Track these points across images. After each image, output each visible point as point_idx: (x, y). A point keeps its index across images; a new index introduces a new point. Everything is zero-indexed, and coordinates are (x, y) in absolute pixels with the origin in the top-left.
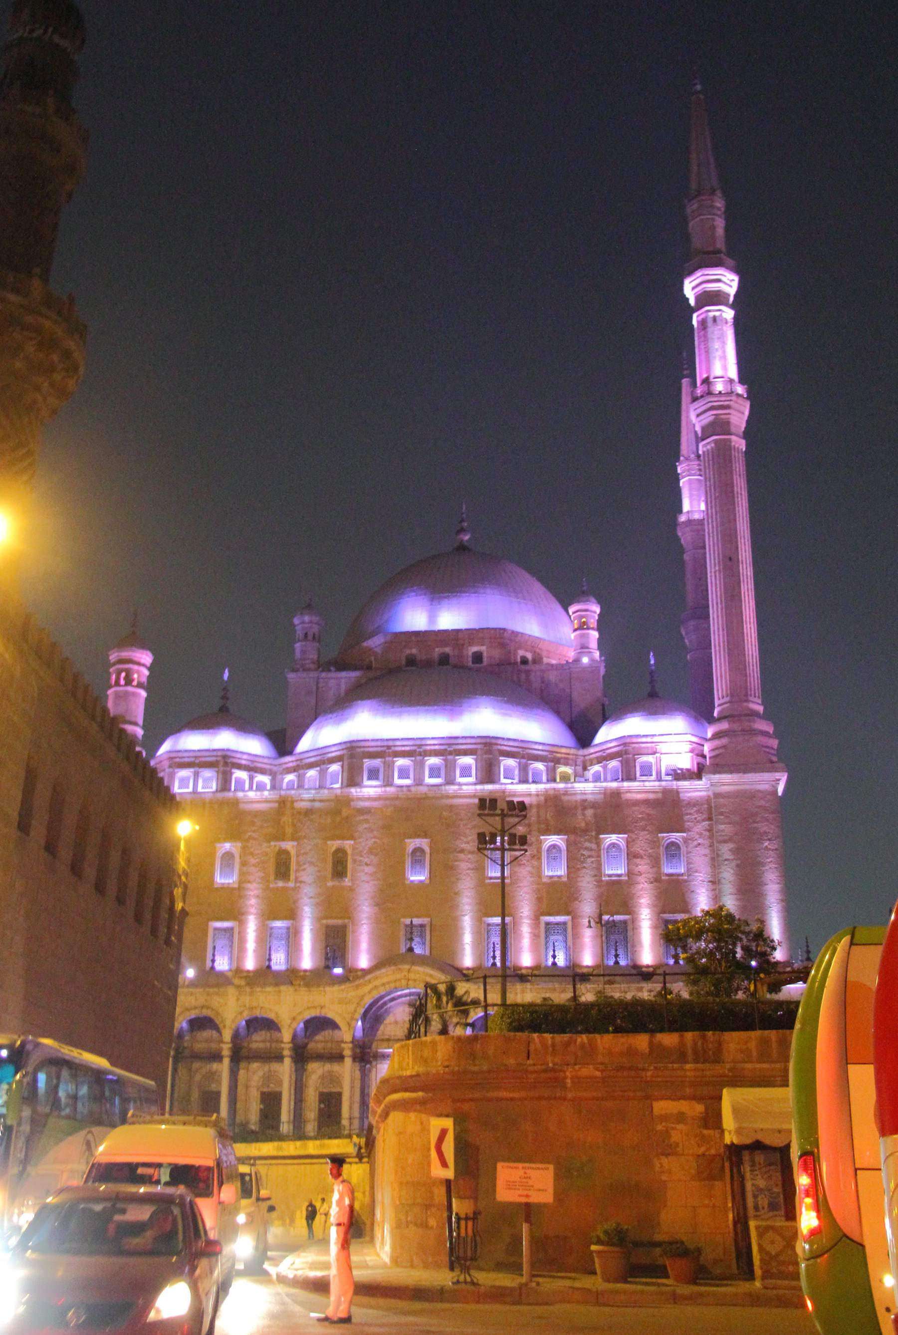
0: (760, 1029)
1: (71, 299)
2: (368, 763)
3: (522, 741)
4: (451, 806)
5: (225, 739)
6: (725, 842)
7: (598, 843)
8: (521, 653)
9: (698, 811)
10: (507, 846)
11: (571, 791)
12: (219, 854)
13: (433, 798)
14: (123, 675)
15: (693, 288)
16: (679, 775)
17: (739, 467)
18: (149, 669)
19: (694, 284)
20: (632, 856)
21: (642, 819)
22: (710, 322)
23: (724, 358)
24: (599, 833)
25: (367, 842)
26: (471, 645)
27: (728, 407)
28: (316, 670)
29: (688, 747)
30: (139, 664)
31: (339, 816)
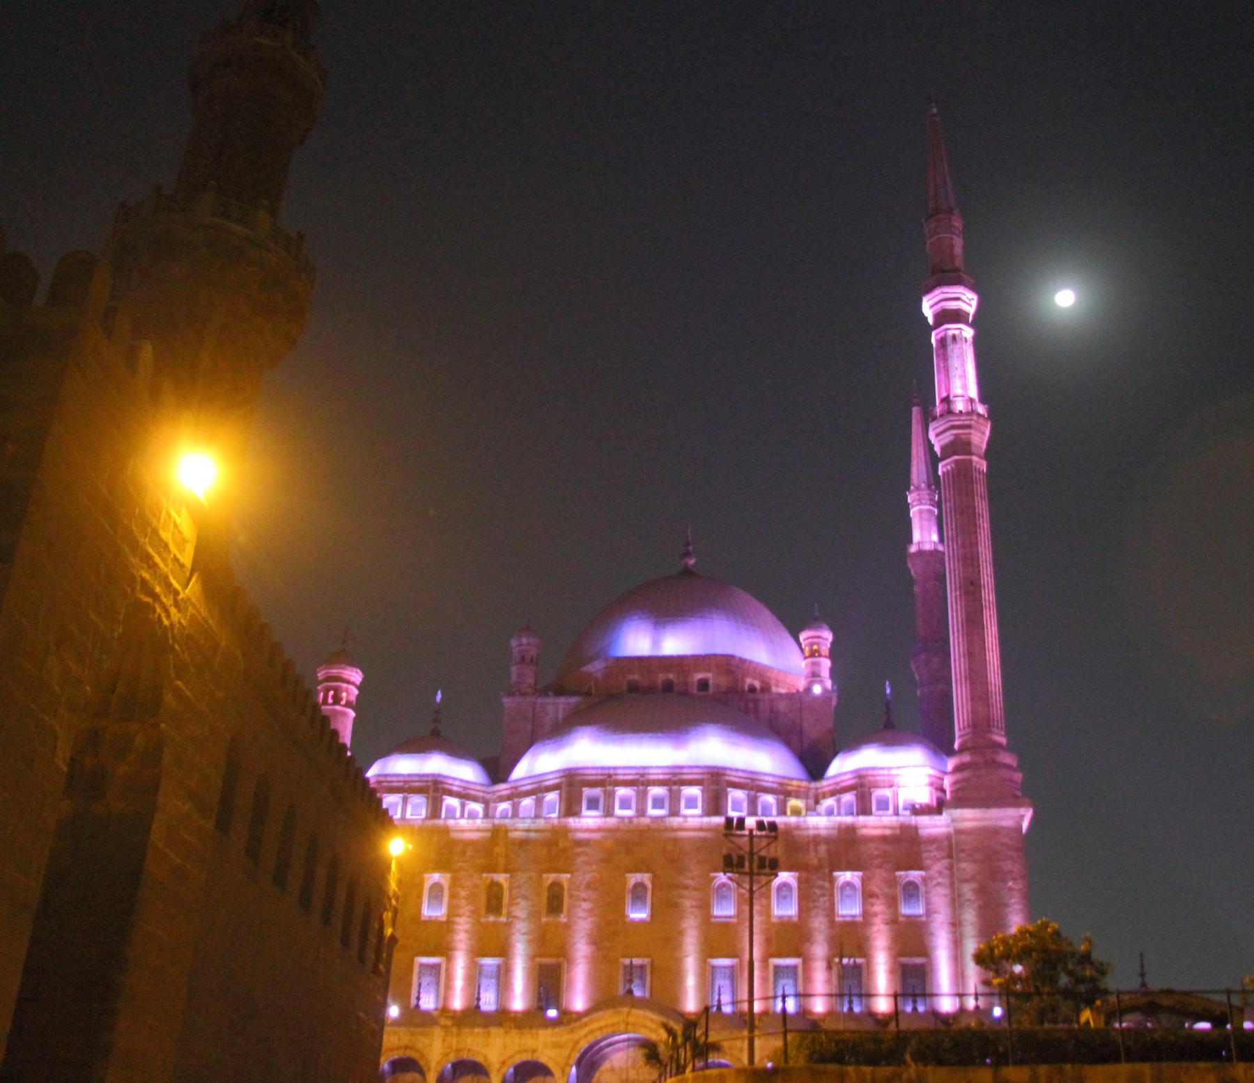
0: (1128, 1061)
1: (301, 237)
2: (587, 792)
3: (752, 772)
4: (675, 840)
5: (436, 764)
6: (967, 881)
7: (832, 881)
8: (749, 681)
9: (937, 849)
10: (756, 871)
11: (803, 825)
12: (427, 885)
13: (657, 830)
14: (332, 693)
15: (931, 307)
16: (917, 810)
17: (981, 488)
18: (359, 688)
19: (931, 302)
20: (868, 896)
21: (877, 857)
22: (949, 341)
23: (964, 376)
24: (831, 871)
25: (586, 874)
26: (697, 671)
27: (969, 427)
28: (534, 694)
29: (927, 780)
30: (348, 682)
31: (556, 848)
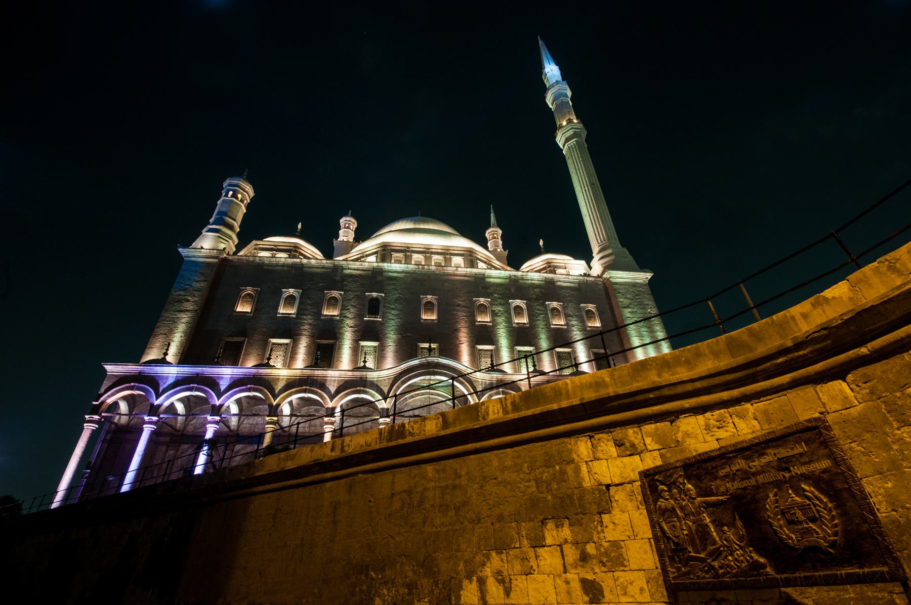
2: (395, 255)
12: (285, 296)
14: (231, 193)
